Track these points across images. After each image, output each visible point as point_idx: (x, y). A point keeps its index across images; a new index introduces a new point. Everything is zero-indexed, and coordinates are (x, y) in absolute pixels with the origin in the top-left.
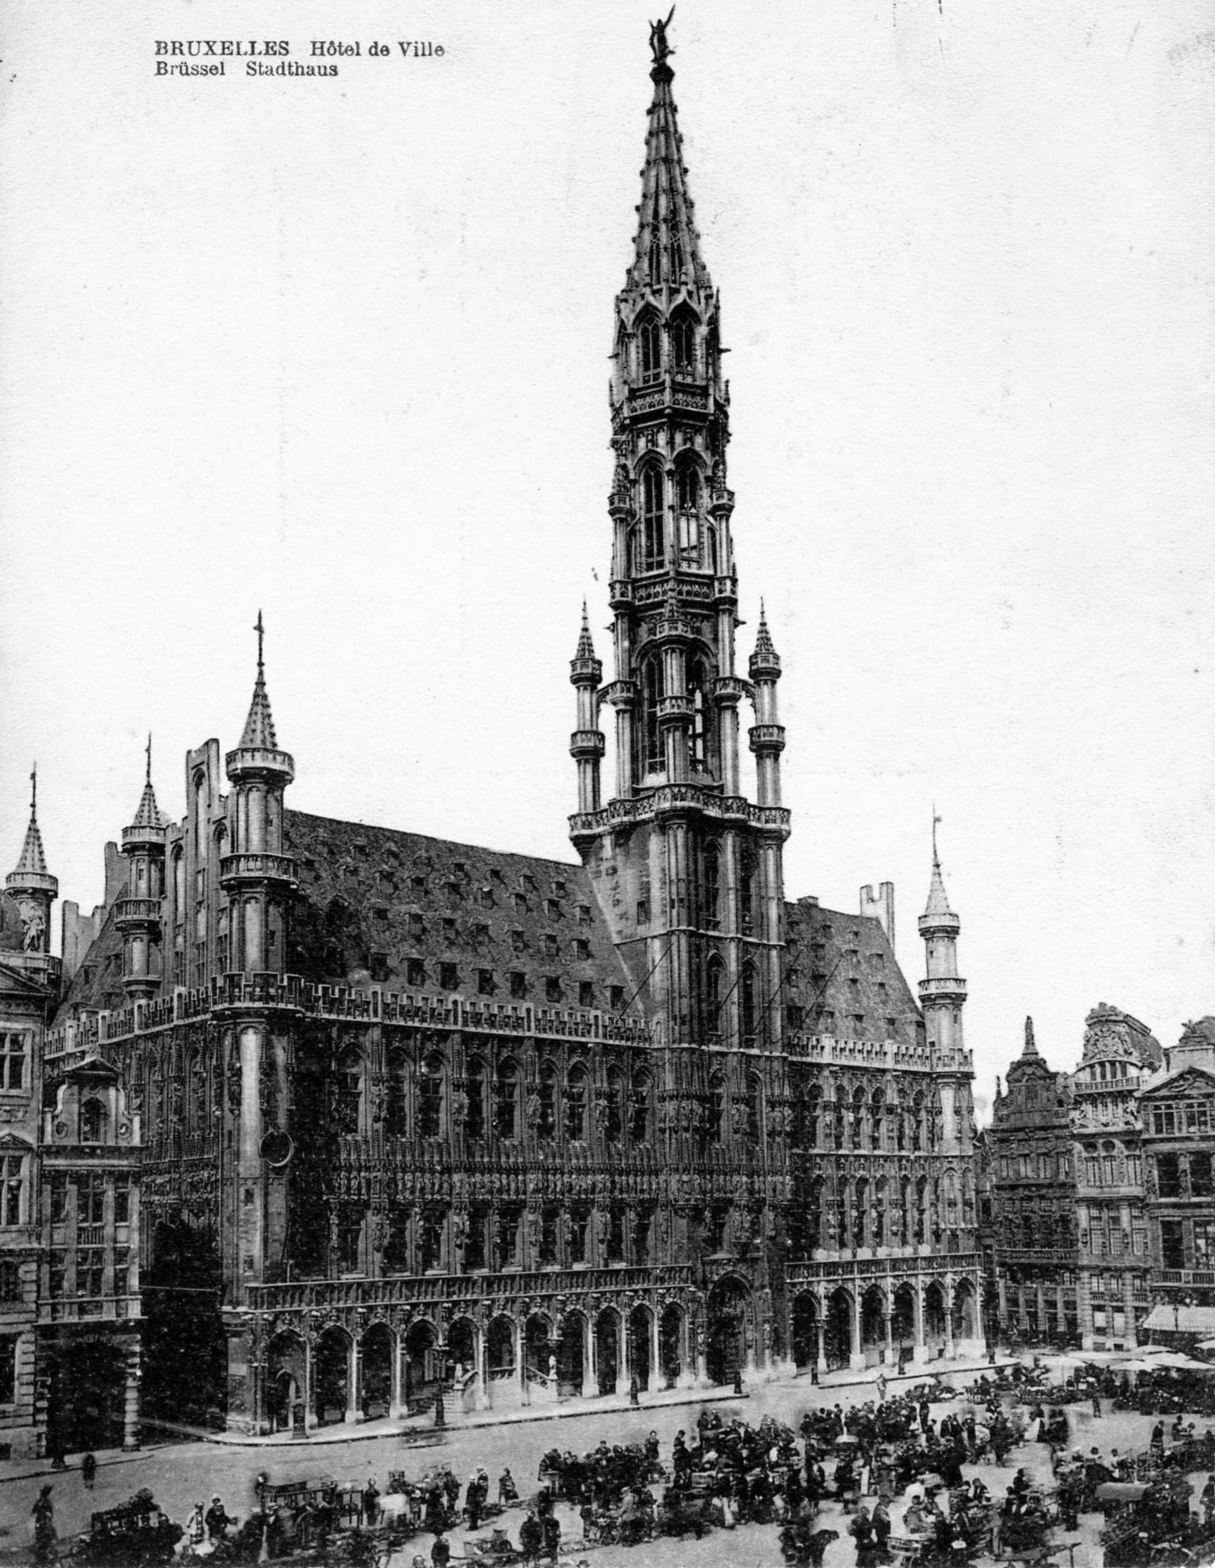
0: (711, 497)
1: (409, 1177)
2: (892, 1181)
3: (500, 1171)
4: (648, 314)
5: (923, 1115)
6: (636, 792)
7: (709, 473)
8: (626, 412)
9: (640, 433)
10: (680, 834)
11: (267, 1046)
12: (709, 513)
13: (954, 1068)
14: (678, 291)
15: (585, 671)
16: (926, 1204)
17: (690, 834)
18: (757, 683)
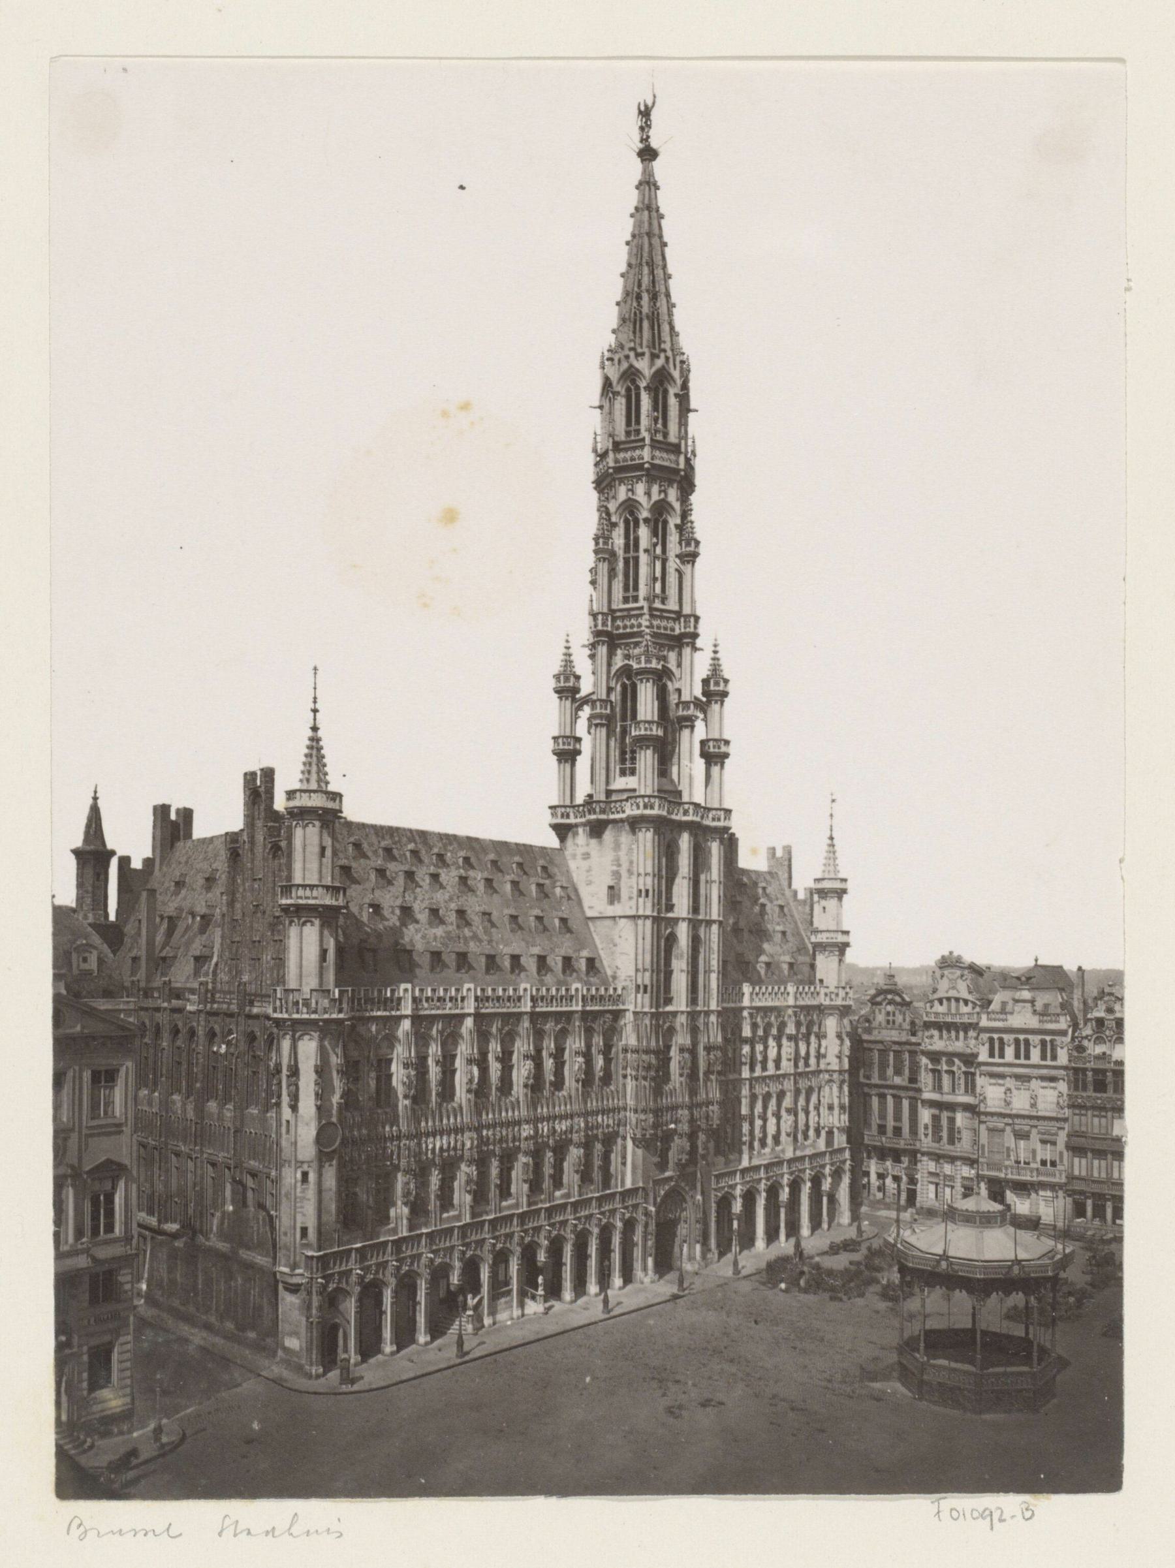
0: (680, 543)
1: (431, 1140)
2: (788, 1094)
3: (502, 1125)
4: (631, 375)
5: (813, 1039)
6: (609, 793)
7: (678, 521)
8: (610, 461)
9: (621, 481)
10: (650, 835)
11: (322, 1050)
12: (677, 556)
13: (839, 1002)
14: (658, 357)
15: (567, 685)
16: (811, 1108)
17: (656, 837)
18: (709, 702)
